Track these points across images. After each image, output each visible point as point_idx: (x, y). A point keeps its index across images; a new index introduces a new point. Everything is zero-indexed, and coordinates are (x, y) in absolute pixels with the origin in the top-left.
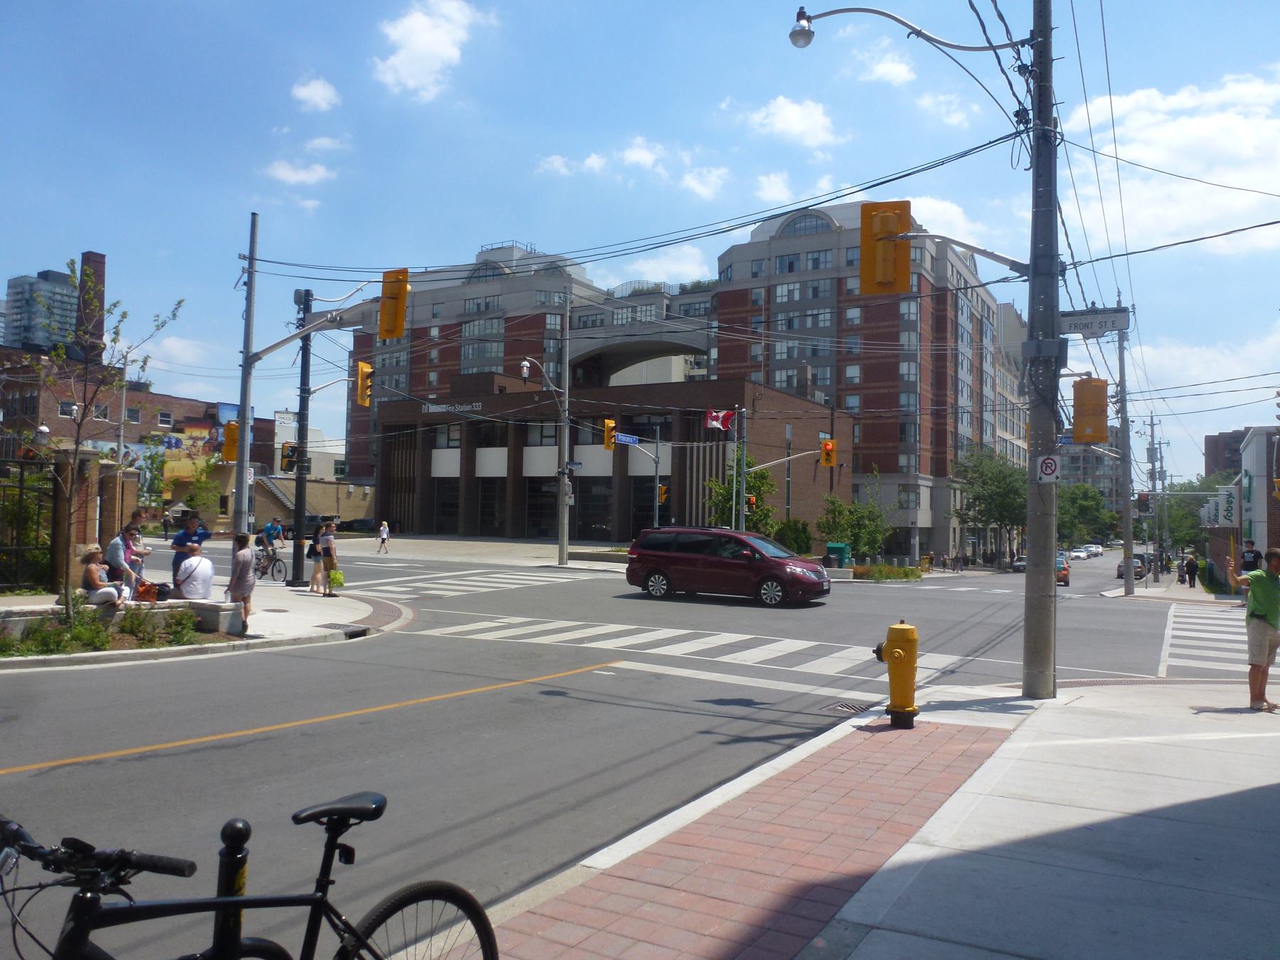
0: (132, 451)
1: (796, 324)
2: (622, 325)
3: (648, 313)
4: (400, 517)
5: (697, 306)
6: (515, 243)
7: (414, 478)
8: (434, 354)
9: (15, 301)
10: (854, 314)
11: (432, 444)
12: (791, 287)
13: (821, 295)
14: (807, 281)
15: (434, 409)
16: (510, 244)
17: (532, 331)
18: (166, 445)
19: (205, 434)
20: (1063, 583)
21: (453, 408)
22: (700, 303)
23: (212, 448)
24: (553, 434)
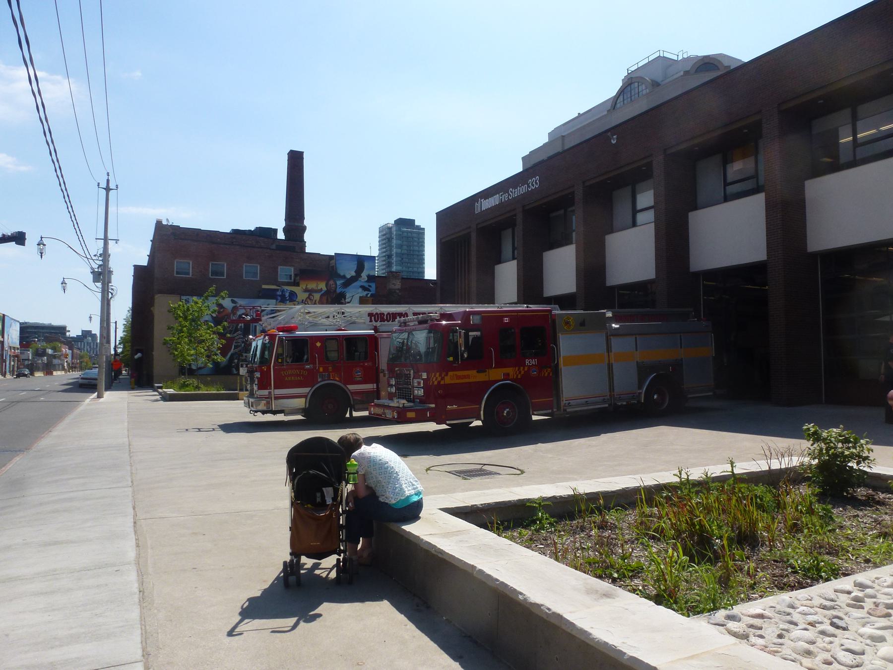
6: (661, 52)
9: (383, 240)
16: (657, 55)
18: (279, 298)
19: (322, 286)
23: (330, 300)
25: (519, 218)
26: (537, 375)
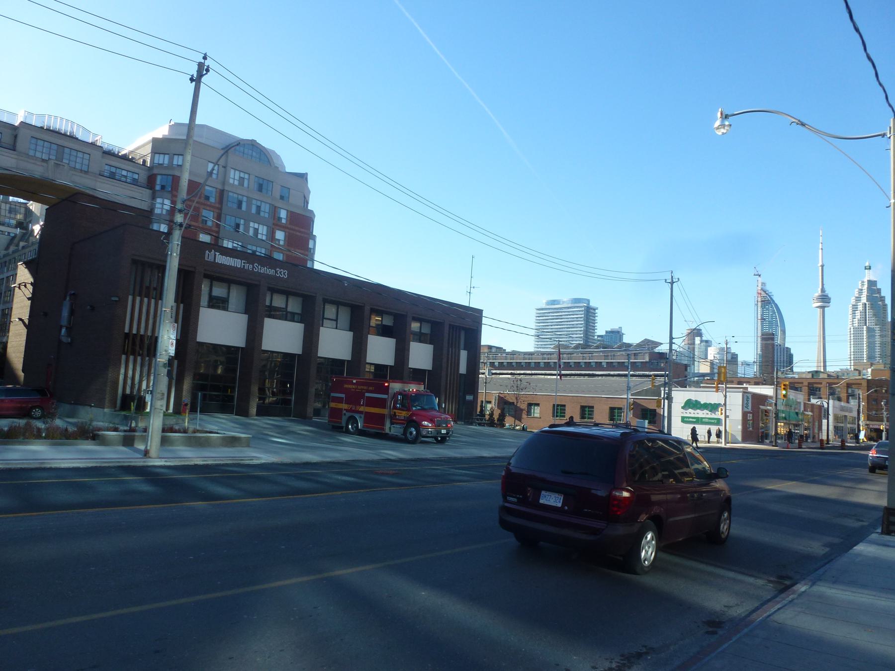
1: (241, 229)
2: (43, 160)
5: (124, 173)
10: (280, 235)
13: (262, 214)
14: (252, 199)
15: (221, 259)
21: (251, 266)
22: (128, 171)
24: (334, 318)
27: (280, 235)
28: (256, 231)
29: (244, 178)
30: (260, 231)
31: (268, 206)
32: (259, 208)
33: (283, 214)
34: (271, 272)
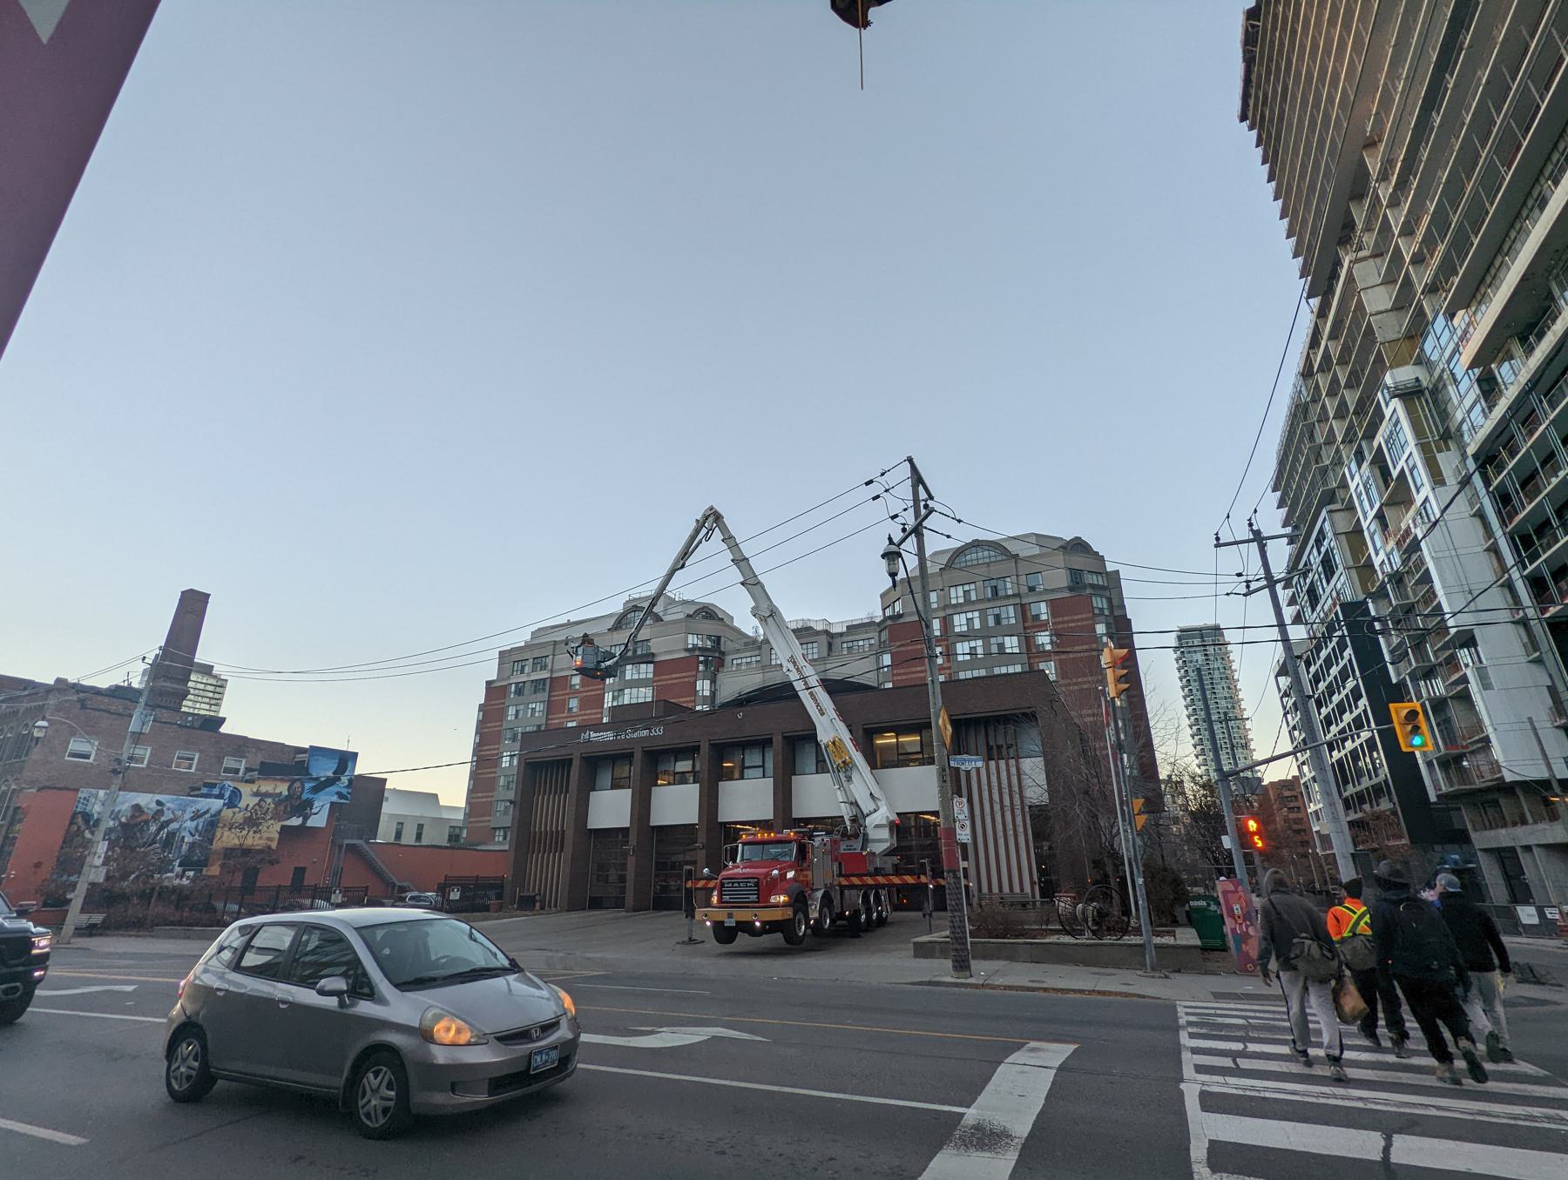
0: (169, 809)
3: (810, 651)
4: (540, 889)
7: (563, 831)
8: (574, 703)
10: (1044, 639)
11: (590, 785)
12: (970, 615)
13: (1004, 622)
17: (683, 674)
20: (1187, 937)
25: (638, 756)
26: (440, 899)
27: (1044, 639)
28: (1001, 646)
29: (969, 591)
30: (1008, 644)
31: (1011, 609)
32: (998, 618)
33: (1043, 610)
34: (645, 733)
